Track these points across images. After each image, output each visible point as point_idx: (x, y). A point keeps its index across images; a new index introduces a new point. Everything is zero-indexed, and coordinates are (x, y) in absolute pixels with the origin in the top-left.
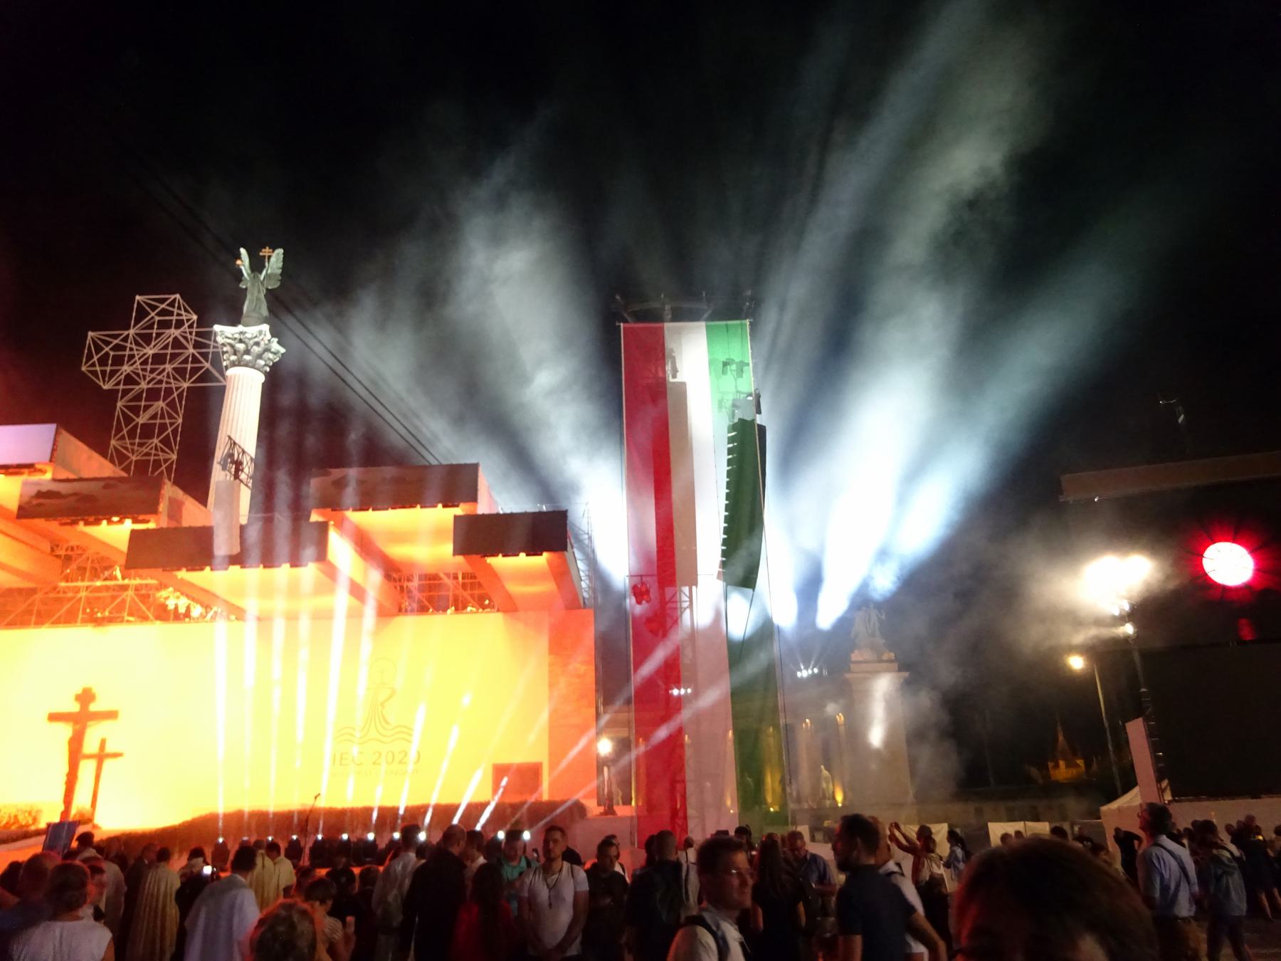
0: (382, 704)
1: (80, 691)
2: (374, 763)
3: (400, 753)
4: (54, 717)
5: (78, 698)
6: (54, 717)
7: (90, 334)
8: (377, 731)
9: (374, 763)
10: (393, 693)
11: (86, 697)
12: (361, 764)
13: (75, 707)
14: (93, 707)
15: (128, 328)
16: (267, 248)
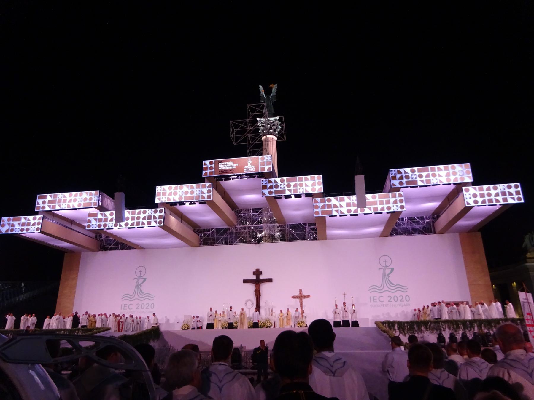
0: (388, 275)
1: (255, 271)
2: (389, 301)
3: (400, 297)
4: (245, 281)
5: (254, 273)
6: (245, 281)
7: (231, 121)
8: (387, 286)
9: (389, 301)
10: (392, 270)
11: (258, 273)
12: (383, 301)
13: (254, 277)
14: (261, 277)
15: (247, 119)
16: (272, 84)
